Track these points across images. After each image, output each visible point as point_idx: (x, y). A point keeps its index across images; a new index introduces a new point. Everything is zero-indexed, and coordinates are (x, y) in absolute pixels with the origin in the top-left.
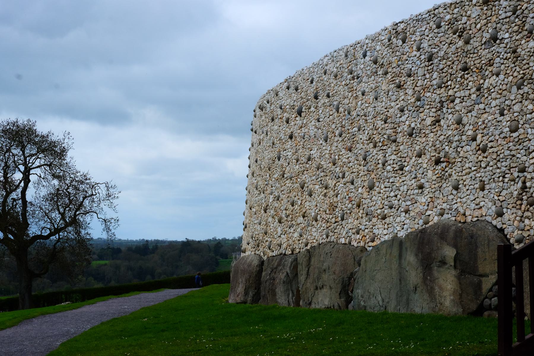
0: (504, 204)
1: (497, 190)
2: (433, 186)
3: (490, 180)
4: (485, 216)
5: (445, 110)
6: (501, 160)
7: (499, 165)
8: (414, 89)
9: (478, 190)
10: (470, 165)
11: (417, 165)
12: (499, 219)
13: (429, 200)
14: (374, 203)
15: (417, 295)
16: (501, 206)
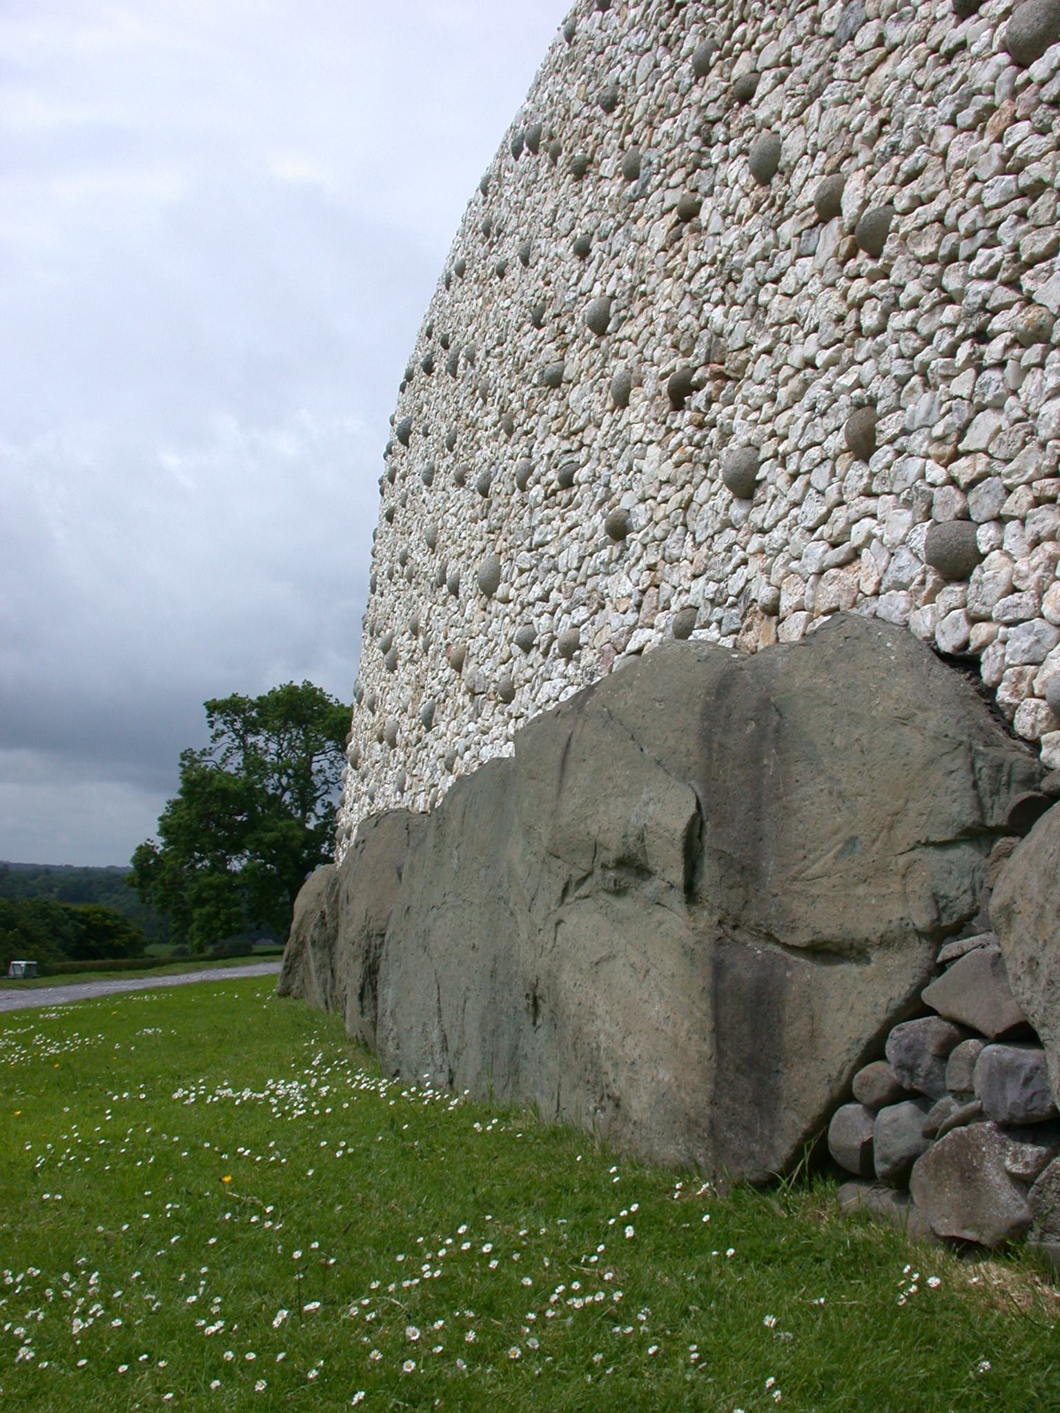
0: (983, 503)
1: (938, 431)
2: (659, 514)
3: (902, 382)
4: (876, 594)
5: (716, 154)
6: (965, 249)
7: (952, 281)
8: (621, 147)
9: (844, 460)
10: (809, 347)
11: (618, 438)
12: (952, 594)
13: (646, 578)
14: (492, 644)
15: (542, 1033)
16: (965, 516)
